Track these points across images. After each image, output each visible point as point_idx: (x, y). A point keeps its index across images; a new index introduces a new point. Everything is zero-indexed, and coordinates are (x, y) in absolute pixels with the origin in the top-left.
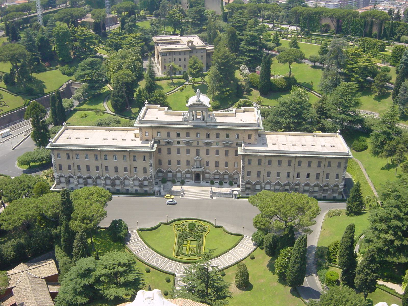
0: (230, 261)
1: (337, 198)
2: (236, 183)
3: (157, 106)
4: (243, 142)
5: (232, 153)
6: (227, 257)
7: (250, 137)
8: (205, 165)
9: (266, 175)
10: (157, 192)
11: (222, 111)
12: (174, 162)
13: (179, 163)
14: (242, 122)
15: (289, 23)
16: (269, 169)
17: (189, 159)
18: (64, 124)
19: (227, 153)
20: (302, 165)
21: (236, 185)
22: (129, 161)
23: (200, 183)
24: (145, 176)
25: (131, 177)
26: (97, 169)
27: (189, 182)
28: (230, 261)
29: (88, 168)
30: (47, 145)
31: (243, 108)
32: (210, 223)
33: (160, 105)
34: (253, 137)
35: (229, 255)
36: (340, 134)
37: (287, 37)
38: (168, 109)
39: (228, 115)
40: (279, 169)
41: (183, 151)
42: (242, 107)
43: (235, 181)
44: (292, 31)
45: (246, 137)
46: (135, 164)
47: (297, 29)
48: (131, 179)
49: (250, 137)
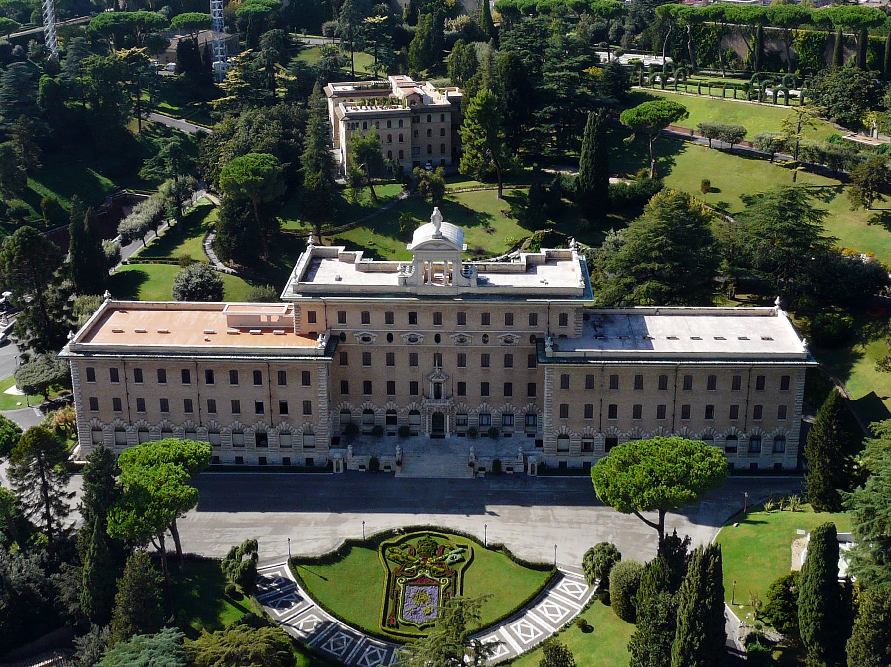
0: (526, 639)
1: (784, 465)
2: (533, 436)
3: (337, 250)
4: (546, 333)
5: (521, 361)
6: (516, 627)
7: (563, 320)
8: (456, 394)
9: (606, 413)
10: (337, 463)
11: (495, 259)
12: (380, 387)
13: (391, 387)
14: (543, 285)
15: (646, 48)
16: (612, 398)
17: (417, 378)
18: (105, 295)
19: (508, 361)
20: (694, 386)
21: (533, 440)
22: (267, 386)
23: (444, 437)
24: (308, 424)
25: (272, 426)
26: (188, 406)
27: (416, 434)
28: (526, 639)
29: (164, 406)
30: (60, 349)
31: (543, 251)
32: (475, 539)
33: (344, 247)
34: (571, 320)
35: (523, 623)
36: (783, 307)
37: (642, 80)
38: (364, 256)
39: (510, 268)
40: (638, 398)
41: (402, 360)
42: (541, 250)
43: (530, 430)
44: (656, 68)
45: (555, 320)
46: (282, 393)
47: (665, 61)
48: (272, 430)
49: (563, 320)
